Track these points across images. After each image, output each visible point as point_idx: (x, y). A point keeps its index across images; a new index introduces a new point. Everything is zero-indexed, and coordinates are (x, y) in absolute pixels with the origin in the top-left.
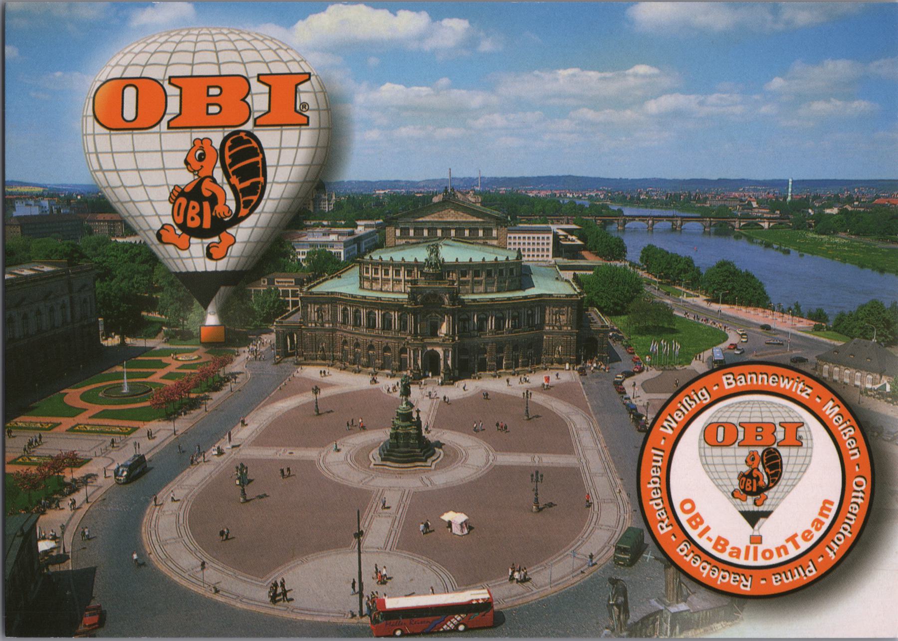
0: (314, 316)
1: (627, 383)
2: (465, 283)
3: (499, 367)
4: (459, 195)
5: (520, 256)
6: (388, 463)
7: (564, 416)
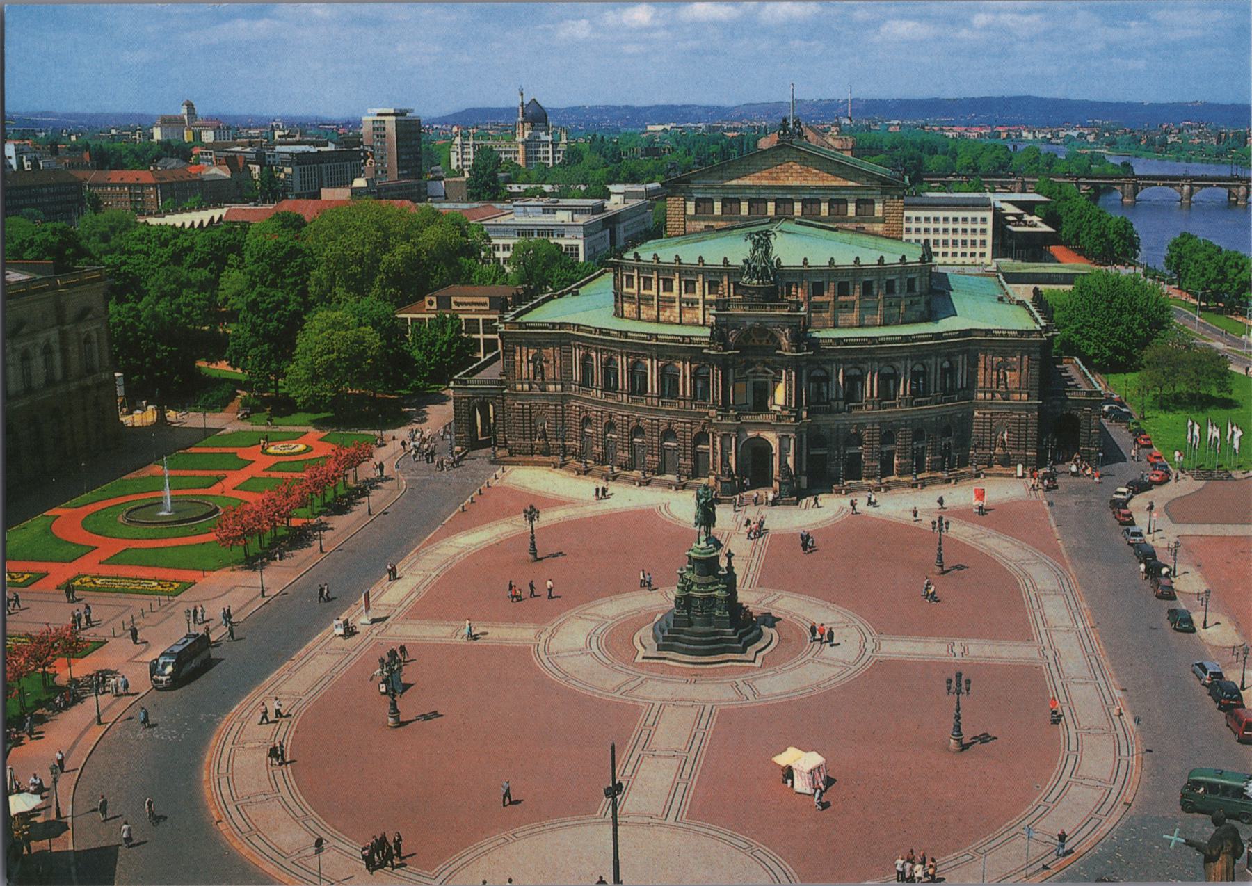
0: (526, 370)
1: (1138, 504)
2: (818, 307)
3: (886, 469)
4: (810, 135)
5: (927, 255)
6: (671, 654)
7: (1012, 568)
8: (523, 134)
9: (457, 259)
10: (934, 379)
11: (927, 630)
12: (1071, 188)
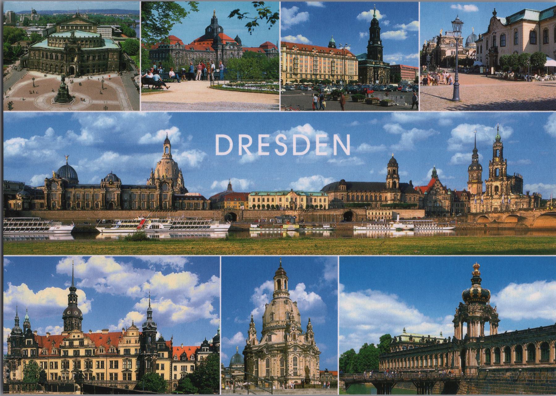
2: (82, 45)
3: (94, 72)
5: (101, 36)
8: (32, 15)
9: (21, 36)
10: (102, 57)
11: (101, 99)
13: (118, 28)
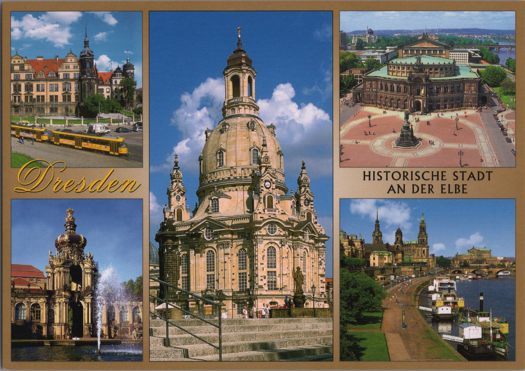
0: (368, 86)
1: (499, 115)
2: (431, 73)
3: (445, 107)
5: (454, 62)
7: (472, 128)
10: (456, 88)
11: (455, 142)
12: (485, 48)
13: (476, 52)
